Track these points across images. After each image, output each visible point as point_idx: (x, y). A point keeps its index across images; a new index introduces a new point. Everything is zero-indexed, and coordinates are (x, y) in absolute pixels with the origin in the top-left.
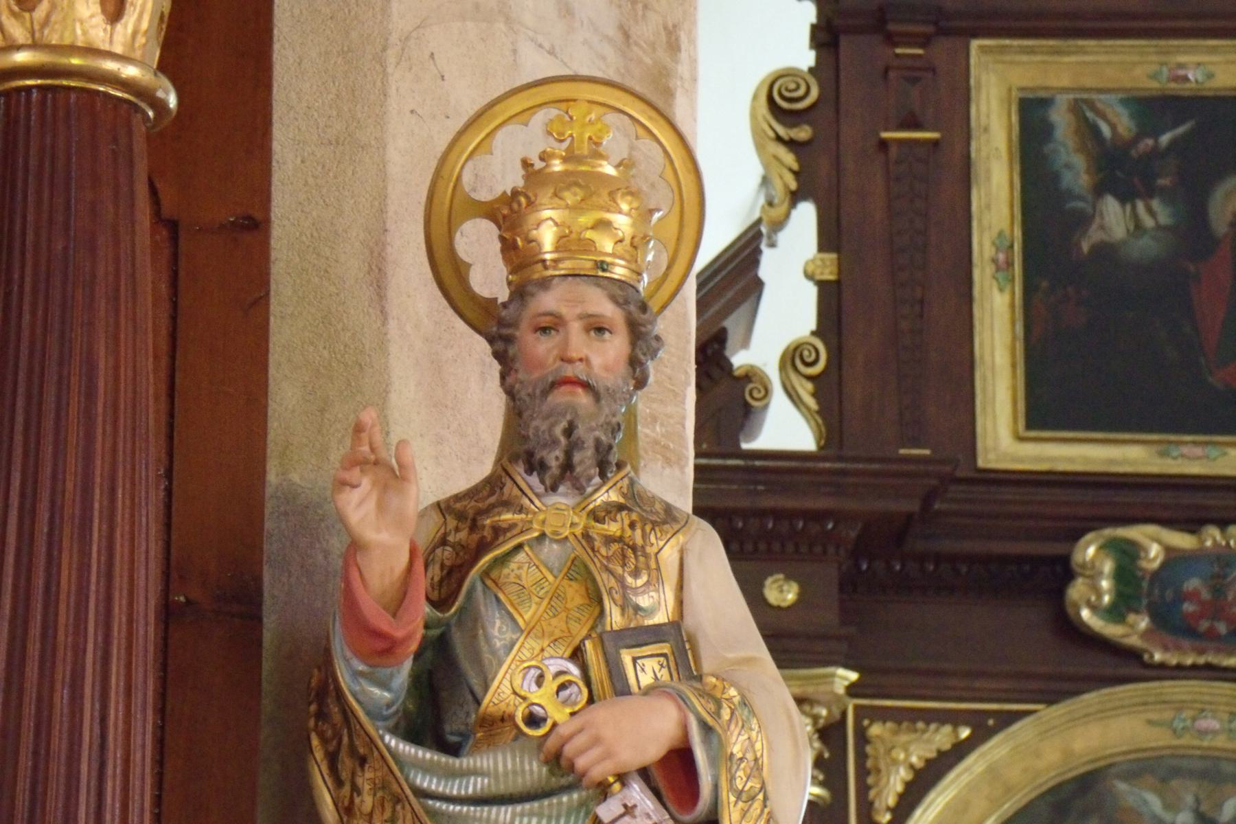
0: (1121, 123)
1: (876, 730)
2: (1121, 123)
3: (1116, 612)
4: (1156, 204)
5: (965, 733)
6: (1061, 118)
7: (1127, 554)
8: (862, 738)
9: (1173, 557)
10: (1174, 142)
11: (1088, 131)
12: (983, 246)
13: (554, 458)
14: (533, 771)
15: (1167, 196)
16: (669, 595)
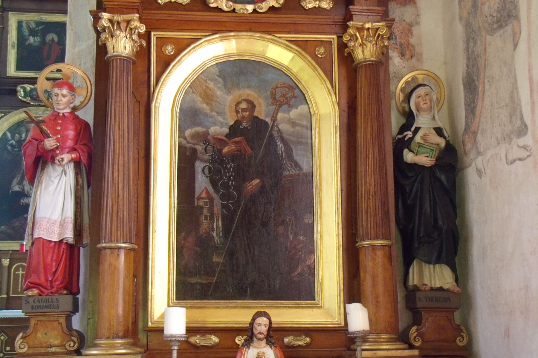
0: (33, 25)
2: (33, 25)
3: (25, 97)
4: (38, 37)
5: (3, 115)
6: (24, 24)
10: (41, 29)
11: (28, 26)
12: (10, 43)
15: (40, 36)
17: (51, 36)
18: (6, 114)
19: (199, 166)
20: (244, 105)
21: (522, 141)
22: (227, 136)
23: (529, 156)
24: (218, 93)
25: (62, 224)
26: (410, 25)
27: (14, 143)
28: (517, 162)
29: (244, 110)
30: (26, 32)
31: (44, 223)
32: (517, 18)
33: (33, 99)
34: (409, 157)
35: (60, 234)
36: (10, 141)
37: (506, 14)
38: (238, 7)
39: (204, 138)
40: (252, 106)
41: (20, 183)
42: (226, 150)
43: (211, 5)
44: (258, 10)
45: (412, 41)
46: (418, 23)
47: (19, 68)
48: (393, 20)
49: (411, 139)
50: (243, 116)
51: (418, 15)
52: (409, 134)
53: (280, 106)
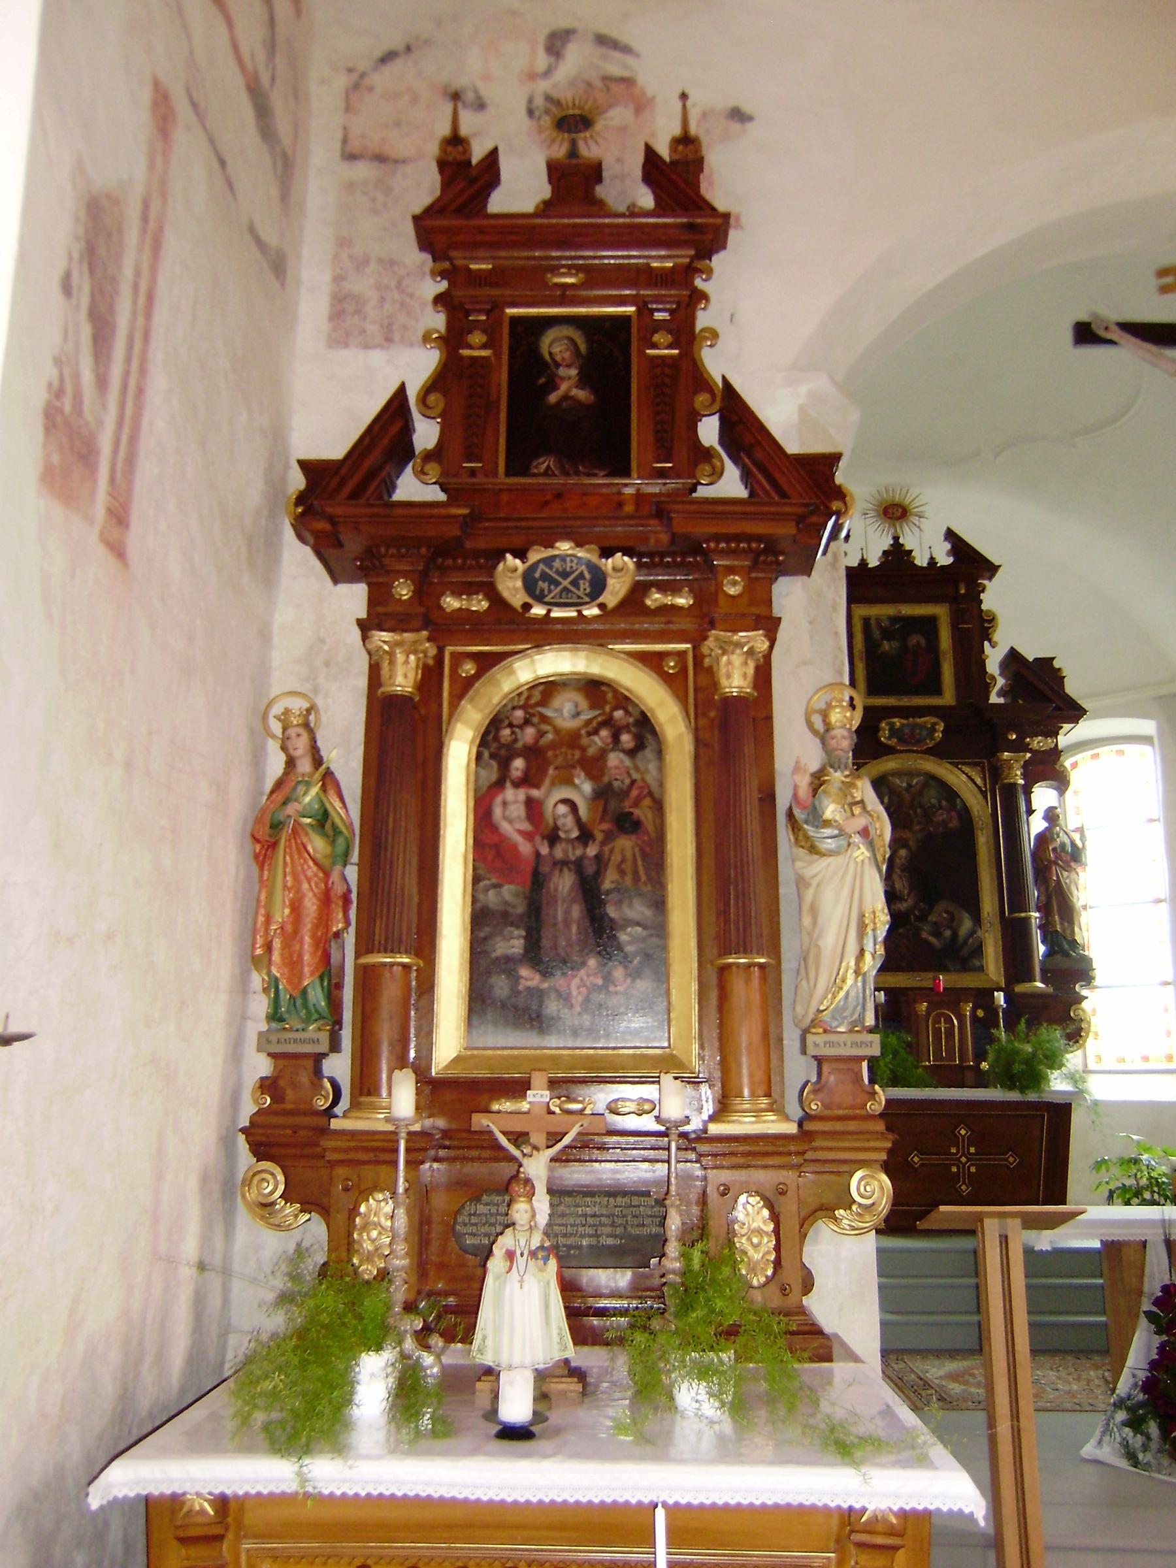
3: (889, 738)
6: (873, 622)
7: (892, 725)
9: (902, 725)
13: (836, 766)
14: (836, 832)
16: (860, 793)
17: (916, 639)
30: (877, 634)
33: (901, 740)
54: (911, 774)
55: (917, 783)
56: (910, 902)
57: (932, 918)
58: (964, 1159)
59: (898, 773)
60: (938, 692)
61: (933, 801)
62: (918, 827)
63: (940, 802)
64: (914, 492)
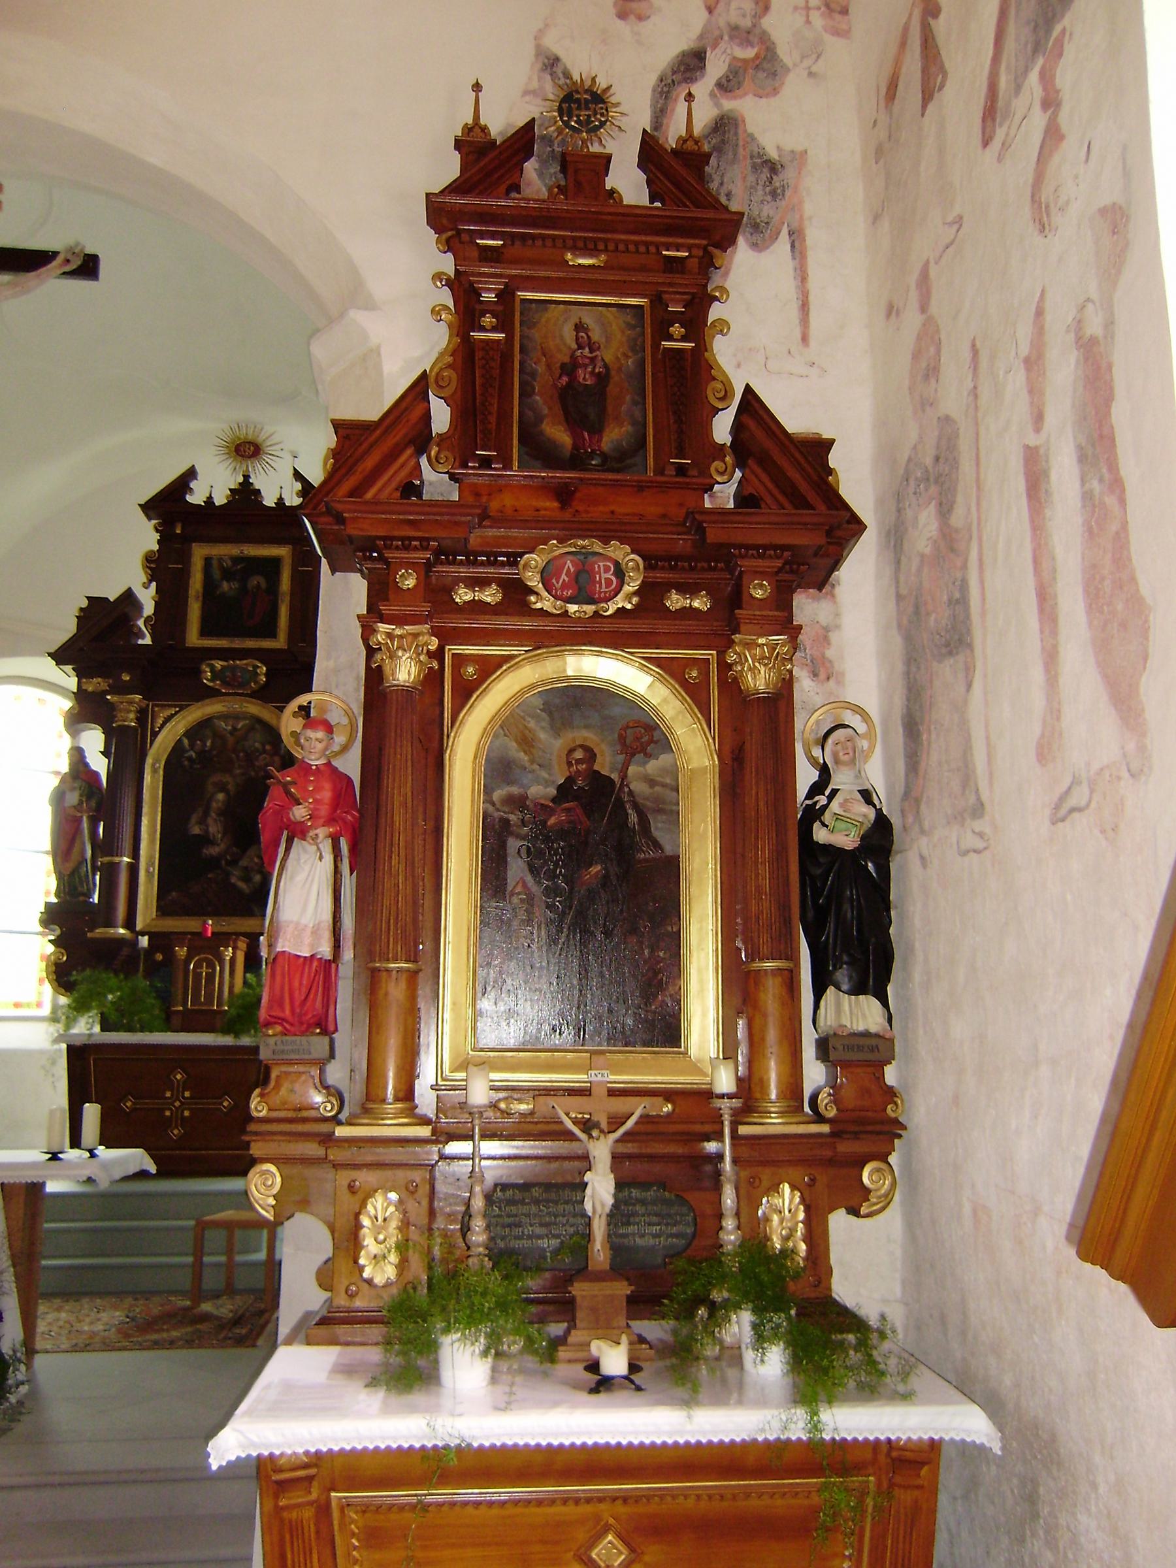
1: (156, 709)
2: (228, 563)
6: (215, 563)
7: (212, 668)
8: (153, 711)
17: (257, 581)
18: (182, 708)
19: (513, 844)
20: (579, 754)
21: (978, 825)
22: (554, 800)
23: (985, 848)
24: (542, 736)
25: (315, 932)
26: (827, 629)
27: (194, 755)
28: (972, 855)
29: (578, 761)
30: (217, 574)
31: (290, 929)
32: (970, 646)
33: (225, 683)
34: (821, 835)
35: (312, 946)
36: (188, 751)
37: (956, 637)
38: (573, 608)
39: (518, 802)
40: (591, 755)
41: (202, 821)
42: (552, 821)
43: (534, 607)
44: (601, 612)
45: (829, 653)
46: (838, 627)
47: (204, 633)
48: (800, 627)
49: (825, 807)
50: (578, 771)
51: (837, 615)
52: (822, 800)
53: (633, 755)
54: (237, 717)
55: (242, 726)
56: (223, 846)
57: (244, 863)
58: (177, 1104)
59: (224, 717)
60: (272, 634)
61: (257, 745)
62: (238, 771)
63: (264, 746)
64: (268, 429)
